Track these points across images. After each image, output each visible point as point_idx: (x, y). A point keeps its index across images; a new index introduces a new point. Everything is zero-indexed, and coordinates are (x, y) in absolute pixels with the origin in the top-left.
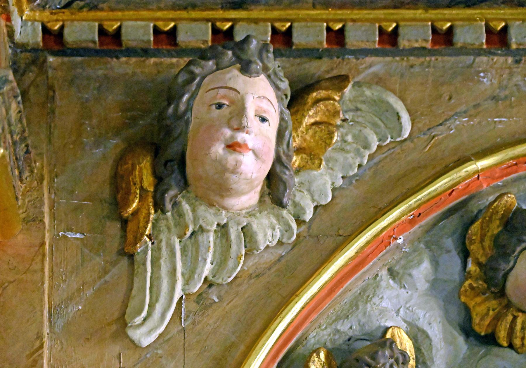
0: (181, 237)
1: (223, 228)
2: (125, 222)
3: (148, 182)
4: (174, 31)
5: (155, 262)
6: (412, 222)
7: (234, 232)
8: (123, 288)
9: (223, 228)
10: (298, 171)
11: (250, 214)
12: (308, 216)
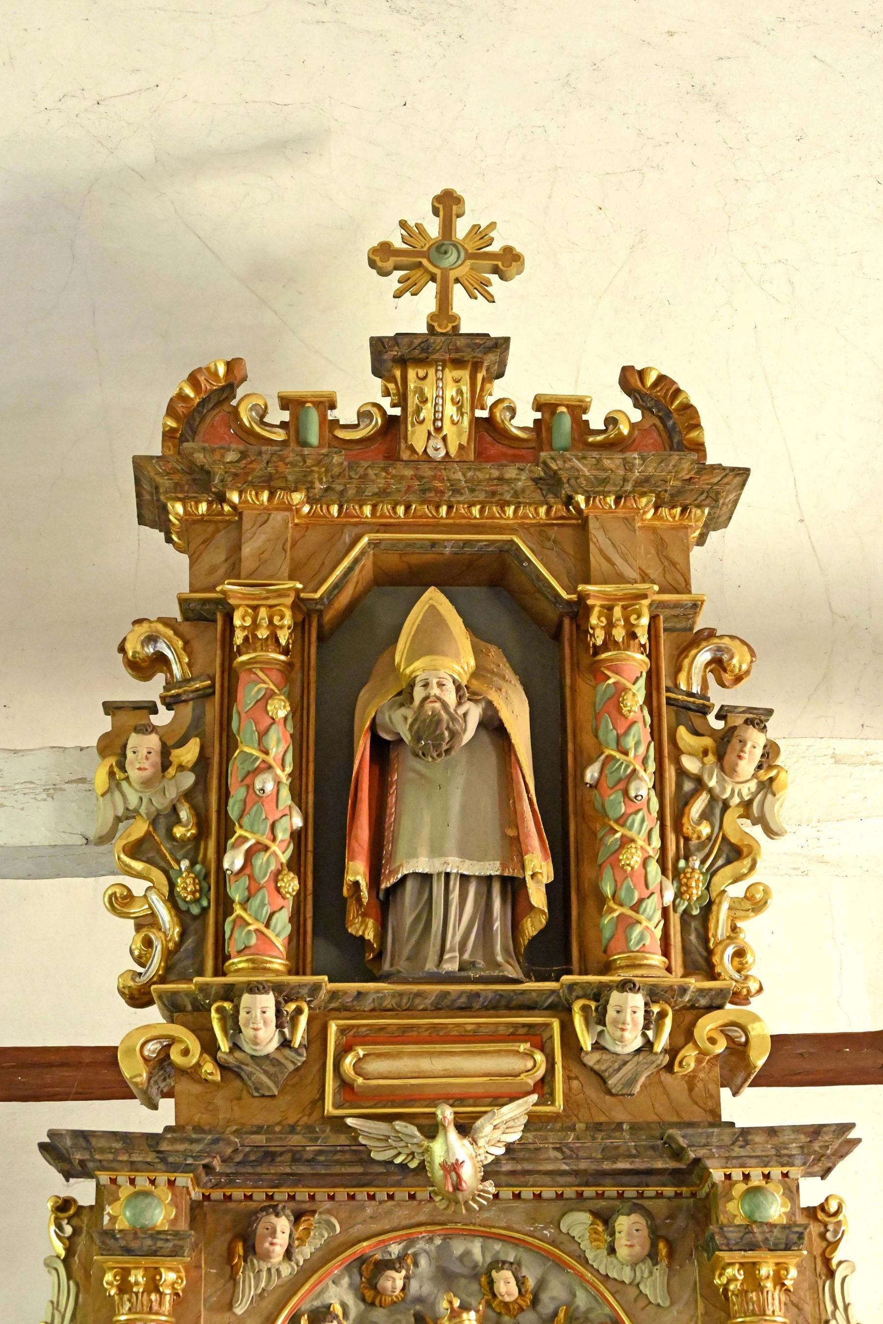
0: (253, 1272)
1: (269, 1270)
2: (232, 1267)
3: (241, 1252)
4: (251, 1195)
5: (244, 1282)
6: (340, 1265)
7: (273, 1271)
8: (231, 1291)
9: (269, 1270)
10: (298, 1246)
11: (280, 1263)
12: (301, 1263)
